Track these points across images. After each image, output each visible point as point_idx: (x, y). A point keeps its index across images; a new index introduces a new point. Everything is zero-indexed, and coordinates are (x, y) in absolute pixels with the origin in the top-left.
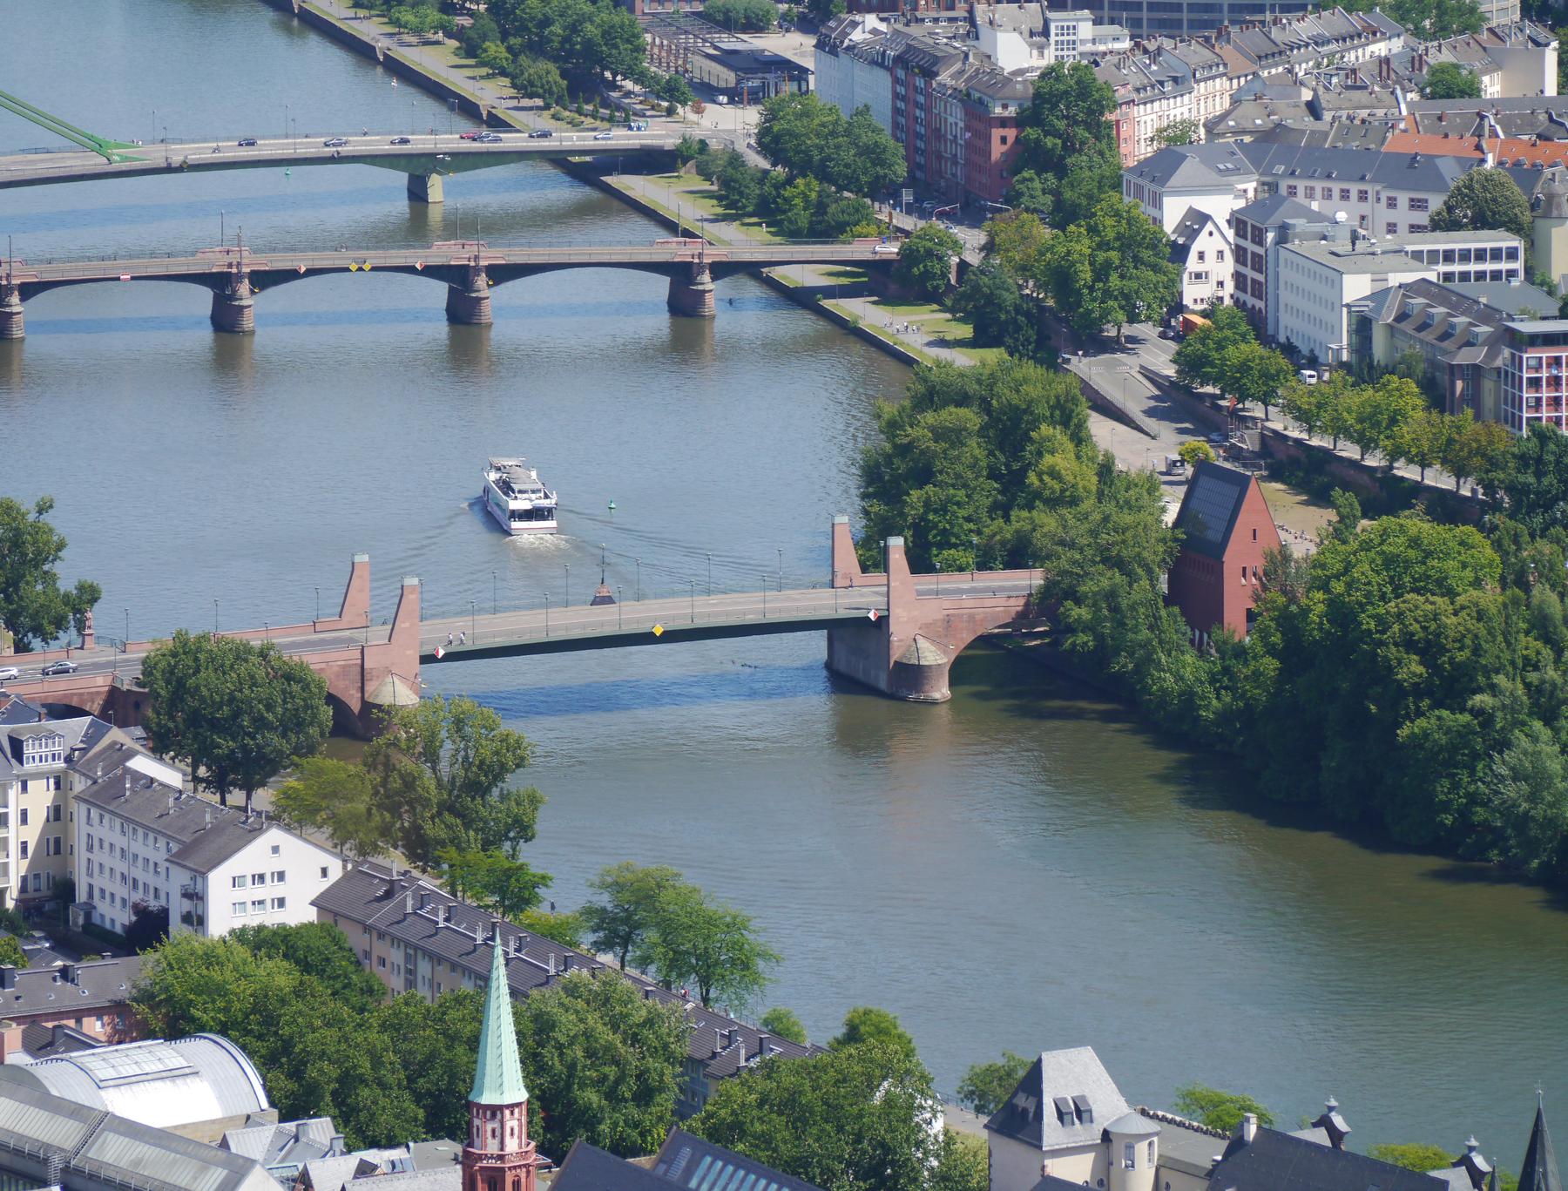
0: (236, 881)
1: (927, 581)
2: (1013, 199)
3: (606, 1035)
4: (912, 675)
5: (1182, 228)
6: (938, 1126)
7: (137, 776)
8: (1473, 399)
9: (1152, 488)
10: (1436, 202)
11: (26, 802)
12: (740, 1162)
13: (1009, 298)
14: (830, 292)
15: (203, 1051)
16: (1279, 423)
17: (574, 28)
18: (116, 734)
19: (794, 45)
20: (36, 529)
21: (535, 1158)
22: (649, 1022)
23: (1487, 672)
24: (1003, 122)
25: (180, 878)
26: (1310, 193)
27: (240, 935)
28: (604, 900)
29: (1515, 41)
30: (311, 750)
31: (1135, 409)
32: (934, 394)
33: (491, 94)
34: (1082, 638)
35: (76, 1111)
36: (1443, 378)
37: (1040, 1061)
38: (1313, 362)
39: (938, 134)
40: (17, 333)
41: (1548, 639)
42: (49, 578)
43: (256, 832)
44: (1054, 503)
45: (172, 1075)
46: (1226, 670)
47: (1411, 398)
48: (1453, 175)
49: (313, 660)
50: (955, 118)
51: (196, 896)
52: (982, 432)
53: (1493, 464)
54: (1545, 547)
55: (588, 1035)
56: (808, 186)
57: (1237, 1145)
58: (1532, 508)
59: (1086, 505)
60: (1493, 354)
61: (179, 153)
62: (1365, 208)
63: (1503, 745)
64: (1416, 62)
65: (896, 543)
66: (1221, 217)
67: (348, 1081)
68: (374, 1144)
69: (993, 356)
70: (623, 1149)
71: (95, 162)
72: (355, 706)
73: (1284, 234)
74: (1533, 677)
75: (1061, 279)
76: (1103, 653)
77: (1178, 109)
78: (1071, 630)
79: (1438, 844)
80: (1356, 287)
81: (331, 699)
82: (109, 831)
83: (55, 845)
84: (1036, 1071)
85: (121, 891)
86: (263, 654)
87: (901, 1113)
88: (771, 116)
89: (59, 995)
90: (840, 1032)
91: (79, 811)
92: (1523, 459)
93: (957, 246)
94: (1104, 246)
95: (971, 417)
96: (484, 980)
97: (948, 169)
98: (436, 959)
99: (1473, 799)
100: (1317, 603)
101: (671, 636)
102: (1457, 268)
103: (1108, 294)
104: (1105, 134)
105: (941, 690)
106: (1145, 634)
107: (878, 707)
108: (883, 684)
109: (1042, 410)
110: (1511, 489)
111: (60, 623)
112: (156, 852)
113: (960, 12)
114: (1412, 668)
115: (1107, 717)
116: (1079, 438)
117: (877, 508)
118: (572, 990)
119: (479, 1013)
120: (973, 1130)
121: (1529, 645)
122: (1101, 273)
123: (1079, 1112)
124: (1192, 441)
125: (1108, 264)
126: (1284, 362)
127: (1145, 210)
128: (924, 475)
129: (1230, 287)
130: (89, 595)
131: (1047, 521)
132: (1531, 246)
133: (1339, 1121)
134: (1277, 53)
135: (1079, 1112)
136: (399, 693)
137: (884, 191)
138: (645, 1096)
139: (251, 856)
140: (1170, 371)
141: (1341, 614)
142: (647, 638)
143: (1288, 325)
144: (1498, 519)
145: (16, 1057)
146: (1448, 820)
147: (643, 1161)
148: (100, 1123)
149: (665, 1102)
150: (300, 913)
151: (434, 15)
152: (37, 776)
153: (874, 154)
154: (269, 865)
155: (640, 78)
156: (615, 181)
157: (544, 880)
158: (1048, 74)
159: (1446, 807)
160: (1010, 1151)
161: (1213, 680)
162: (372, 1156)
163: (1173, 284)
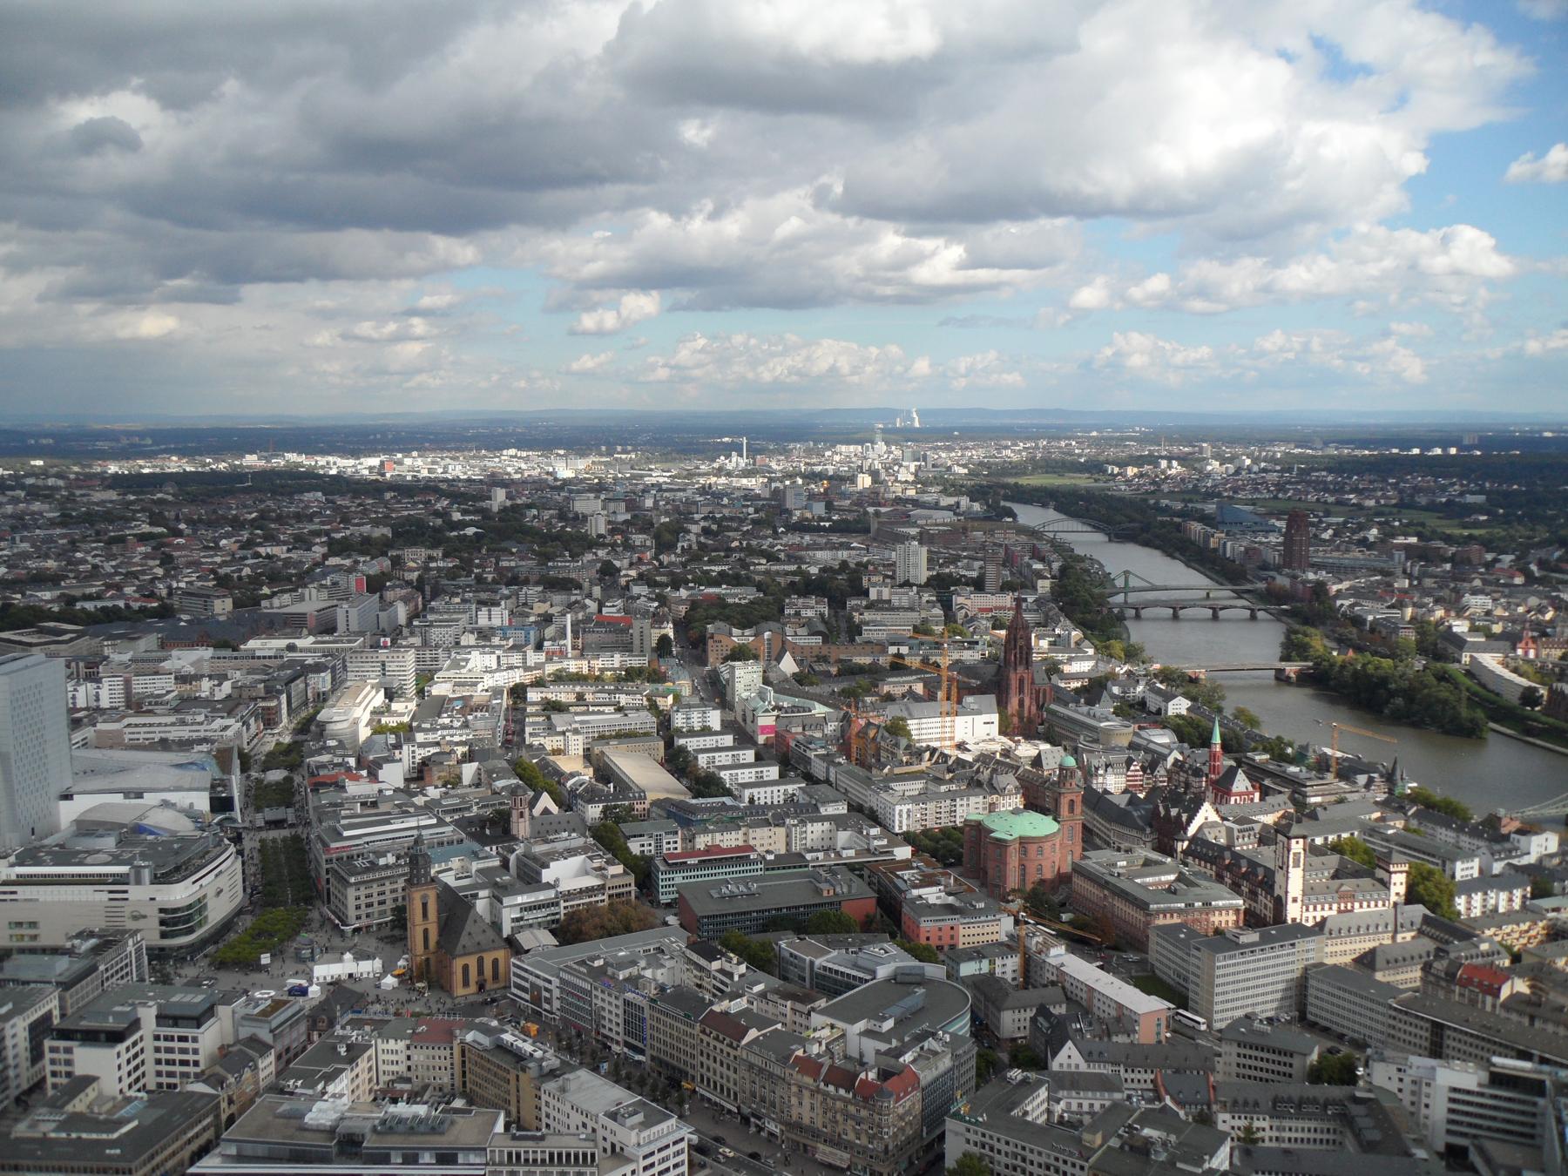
15: (1167, 731)
77: (1340, 586)
139: (1175, 701)
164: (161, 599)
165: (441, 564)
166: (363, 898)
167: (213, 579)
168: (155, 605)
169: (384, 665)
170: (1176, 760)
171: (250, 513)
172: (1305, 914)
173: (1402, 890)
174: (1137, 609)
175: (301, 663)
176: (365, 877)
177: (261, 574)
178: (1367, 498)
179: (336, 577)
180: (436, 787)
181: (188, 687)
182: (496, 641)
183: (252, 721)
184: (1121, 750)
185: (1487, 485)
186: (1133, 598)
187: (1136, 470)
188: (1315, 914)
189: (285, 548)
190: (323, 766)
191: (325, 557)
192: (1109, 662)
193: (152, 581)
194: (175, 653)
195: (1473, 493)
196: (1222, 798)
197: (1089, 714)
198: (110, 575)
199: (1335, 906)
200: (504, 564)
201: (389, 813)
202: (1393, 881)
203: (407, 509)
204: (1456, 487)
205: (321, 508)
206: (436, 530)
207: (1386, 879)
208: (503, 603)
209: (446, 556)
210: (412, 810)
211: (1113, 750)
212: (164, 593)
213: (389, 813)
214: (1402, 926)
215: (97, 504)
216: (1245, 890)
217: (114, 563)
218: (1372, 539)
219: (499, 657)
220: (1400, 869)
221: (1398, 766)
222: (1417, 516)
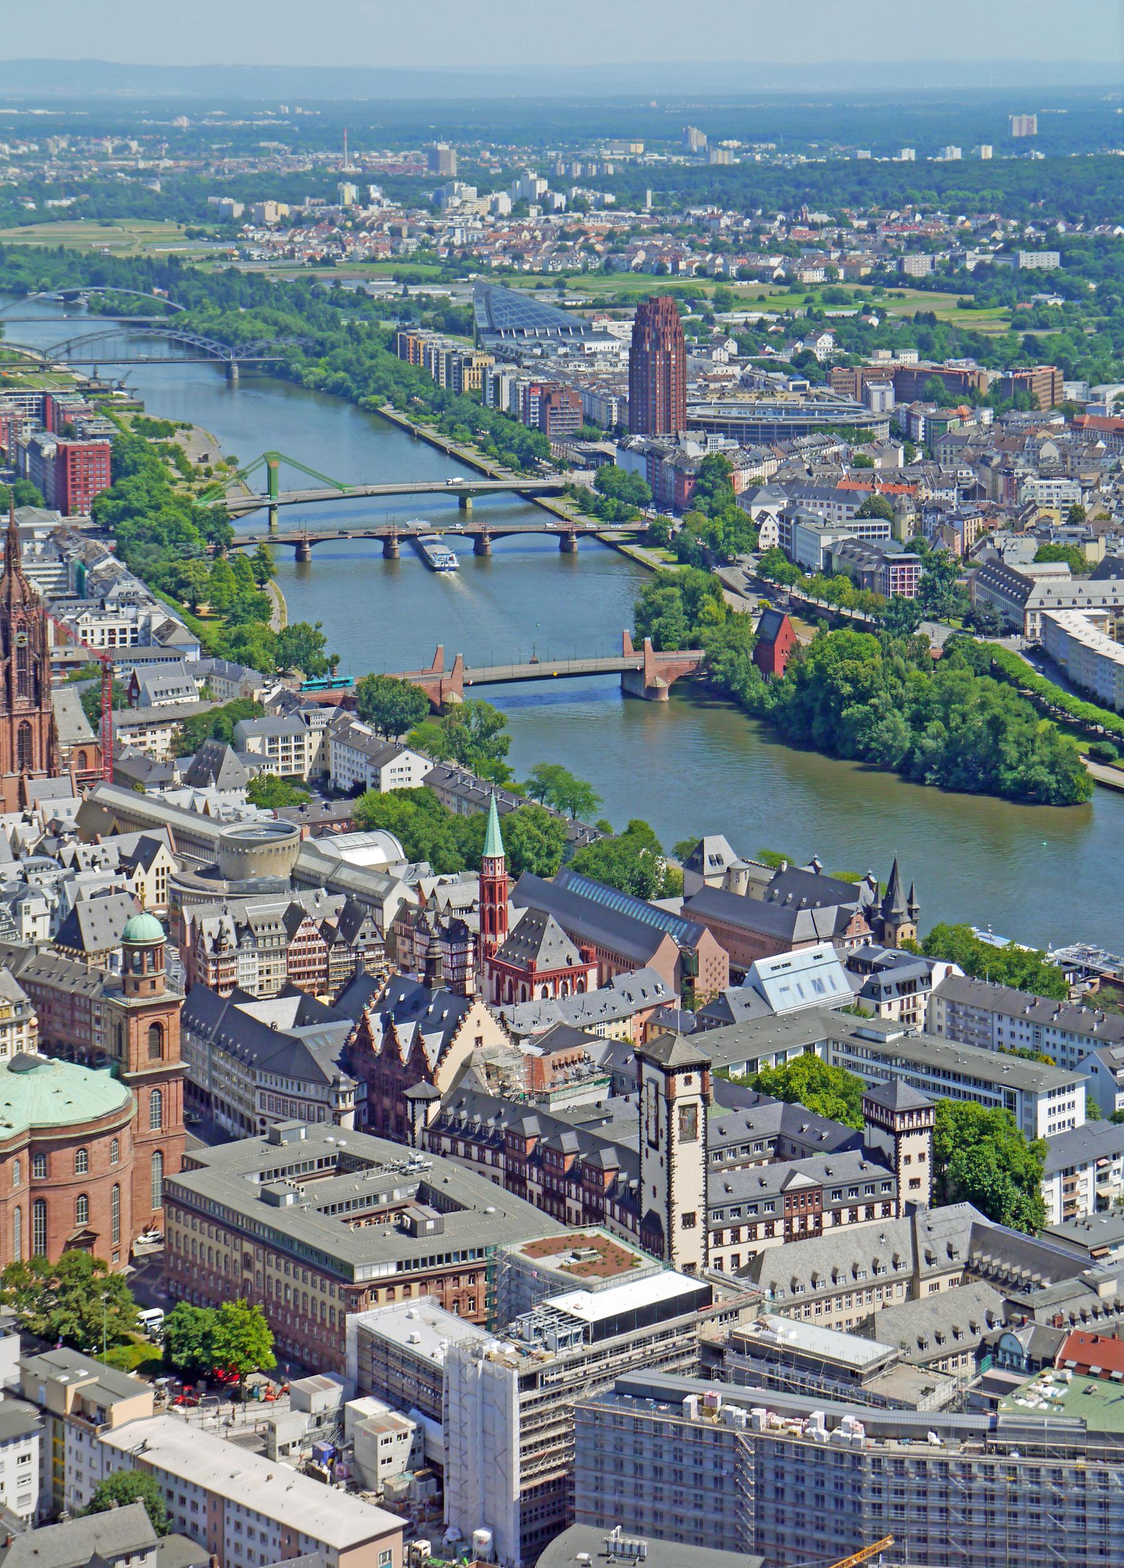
0: (392, 771)
1: (660, 655)
2: (693, 507)
3: (536, 832)
4: (653, 692)
5: (758, 518)
6: (664, 866)
7: (354, 730)
8: (871, 584)
9: (747, 617)
10: (857, 508)
11: (311, 740)
12: (587, 880)
13: (692, 545)
14: (623, 543)
15: (378, 836)
16: (797, 593)
17: (523, 441)
18: (346, 714)
19: (609, 447)
20: (315, 635)
21: (508, 878)
22: (552, 826)
23: (877, 690)
24: (689, 477)
25: (371, 770)
26: (808, 505)
27: (394, 791)
28: (534, 778)
29: (887, 446)
30: (421, 720)
31: (741, 588)
32: (662, 583)
33: (491, 466)
34: (720, 677)
35: (330, 859)
36: (859, 576)
37: (702, 842)
38: (809, 570)
39: (664, 481)
40: (308, 559)
41: (899, 677)
42: (320, 653)
43: (399, 752)
44: (709, 624)
45: (367, 846)
46: (776, 690)
47: (846, 583)
48: (863, 497)
49: (423, 684)
50: (671, 475)
51: (377, 776)
52: (681, 597)
53: (879, 609)
54: (899, 642)
55: (528, 831)
56: (614, 502)
57: (779, 873)
58: (894, 626)
59: (722, 625)
60: (878, 567)
61: (370, 489)
62: (829, 510)
63: (882, 718)
64: (849, 454)
65: (648, 640)
66: (774, 515)
67: (436, 848)
68: (445, 872)
69: (686, 567)
70: (541, 874)
71: (338, 493)
72: (438, 703)
73: (798, 520)
74: (894, 692)
75: (712, 538)
76: (728, 683)
77: (758, 472)
78: (715, 673)
79: (858, 756)
80: (826, 541)
81: (430, 701)
82: (343, 751)
83: (323, 757)
84: (702, 844)
85: (348, 775)
86: (403, 683)
87: (649, 861)
88: (600, 475)
89: (324, 815)
90: (625, 829)
91: (332, 743)
92: (890, 608)
93: (672, 525)
94: (729, 525)
95: (677, 591)
96: (487, 809)
97: (668, 495)
98: (469, 801)
99: (872, 739)
100: (811, 665)
101: (560, 676)
102: (864, 533)
103: (729, 544)
104: (730, 483)
105: (665, 697)
106: (744, 675)
107: (641, 704)
108: (642, 694)
109: (704, 588)
110: (885, 619)
111: (324, 671)
112: (362, 759)
113: (673, 434)
114: (847, 689)
115: (730, 708)
116: (719, 599)
117: (641, 626)
118: (522, 813)
119: (485, 820)
120: (677, 867)
121: (892, 679)
122: (727, 536)
123: (718, 860)
124: (763, 601)
125: (730, 532)
126: (797, 569)
127: (744, 511)
128: (659, 614)
129: (777, 541)
130: (336, 660)
131: (706, 632)
132: (893, 525)
133: (818, 863)
134: (795, 450)
135: (718, 860)
136: (455, 698)
137: (643, 504)
138: (550, 854)
139: (399, 761)
140: (754, 573)
141: (820, 668)
142: (551, 677)
143: (799, 556)
144: (881, 631)
145: (308, 838)
146: (861, 747)
147: (549, 879)
148: (340, 864)
149: (558, 857)
150: (417, 783)
151: (469, 436)
152: (316, 730)
153: (640, 489)
154: (405, 765)
155: (549, 460)
156: (539, 499)
157: (511, 770)
158: (707, 458)
159: (859, 742)
160: (691, 875)
161: (771, 693)
162: (445, 877)
163: (756, 539)
170: (405, 905)
172: (714, 1254)
173: (922, 1170)
174: (298, 544)
178: (809, 265)
184: (275, 889)
185: (1061, 227)
186: (284, 528)
187: (284, 209)
188: (735, 1249)
192: (235, 677)
195: (1034, 246)
196: (512, 987)
197: (193, 809)
199: (779, 1227)
202: (903, 1153)
204: (998, 235)
207: (888, 1149)
211: (254, 890)
214: (929, 1261)
216: (575, 1205)
218: (821, 356)
220: (916, 1123)
221: (900, 881)
222: (917, 302)
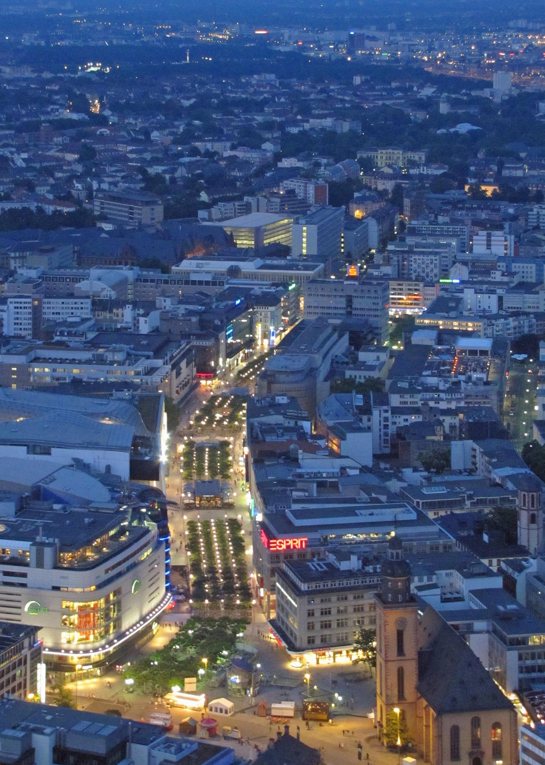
164: (78, 202)
165: (425, 171)
166: (317, 614)
167: (142, 180)
168: (72, 209)
169: (349, 300)
171: (188, 99)
175: (246, 294)
176: (321, 585)
177: (200, 176)
179: (289, 184)
180: (415, 470)
181: (108, 315)
182: (497, 276)
183: (183, 364)
189: (228, 144)
190: (270, 429)
191: (278, 157)
193: (69, 180)
194: (95, 272)
198: (20, 170)
200: (506, 173)
201: (354, 501)
203: (381, 97)
205: (274, 95)
206: (423, 126)
208: (507, 225)
209: (429, 162)
210: (383, 498)
212: (83, 195)
213: (354, 501)
215: (9, 82)
217: (25, 156)
219: (500, 299)
